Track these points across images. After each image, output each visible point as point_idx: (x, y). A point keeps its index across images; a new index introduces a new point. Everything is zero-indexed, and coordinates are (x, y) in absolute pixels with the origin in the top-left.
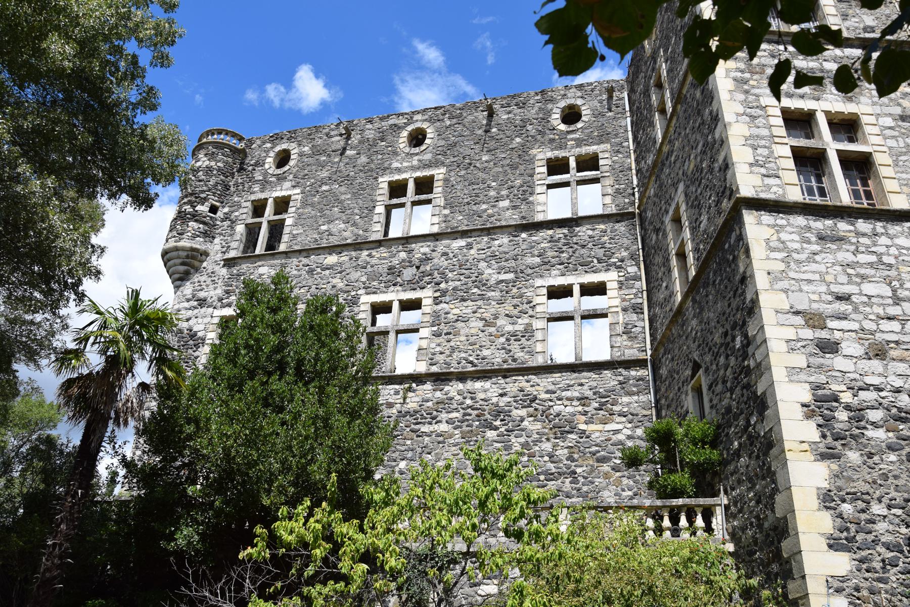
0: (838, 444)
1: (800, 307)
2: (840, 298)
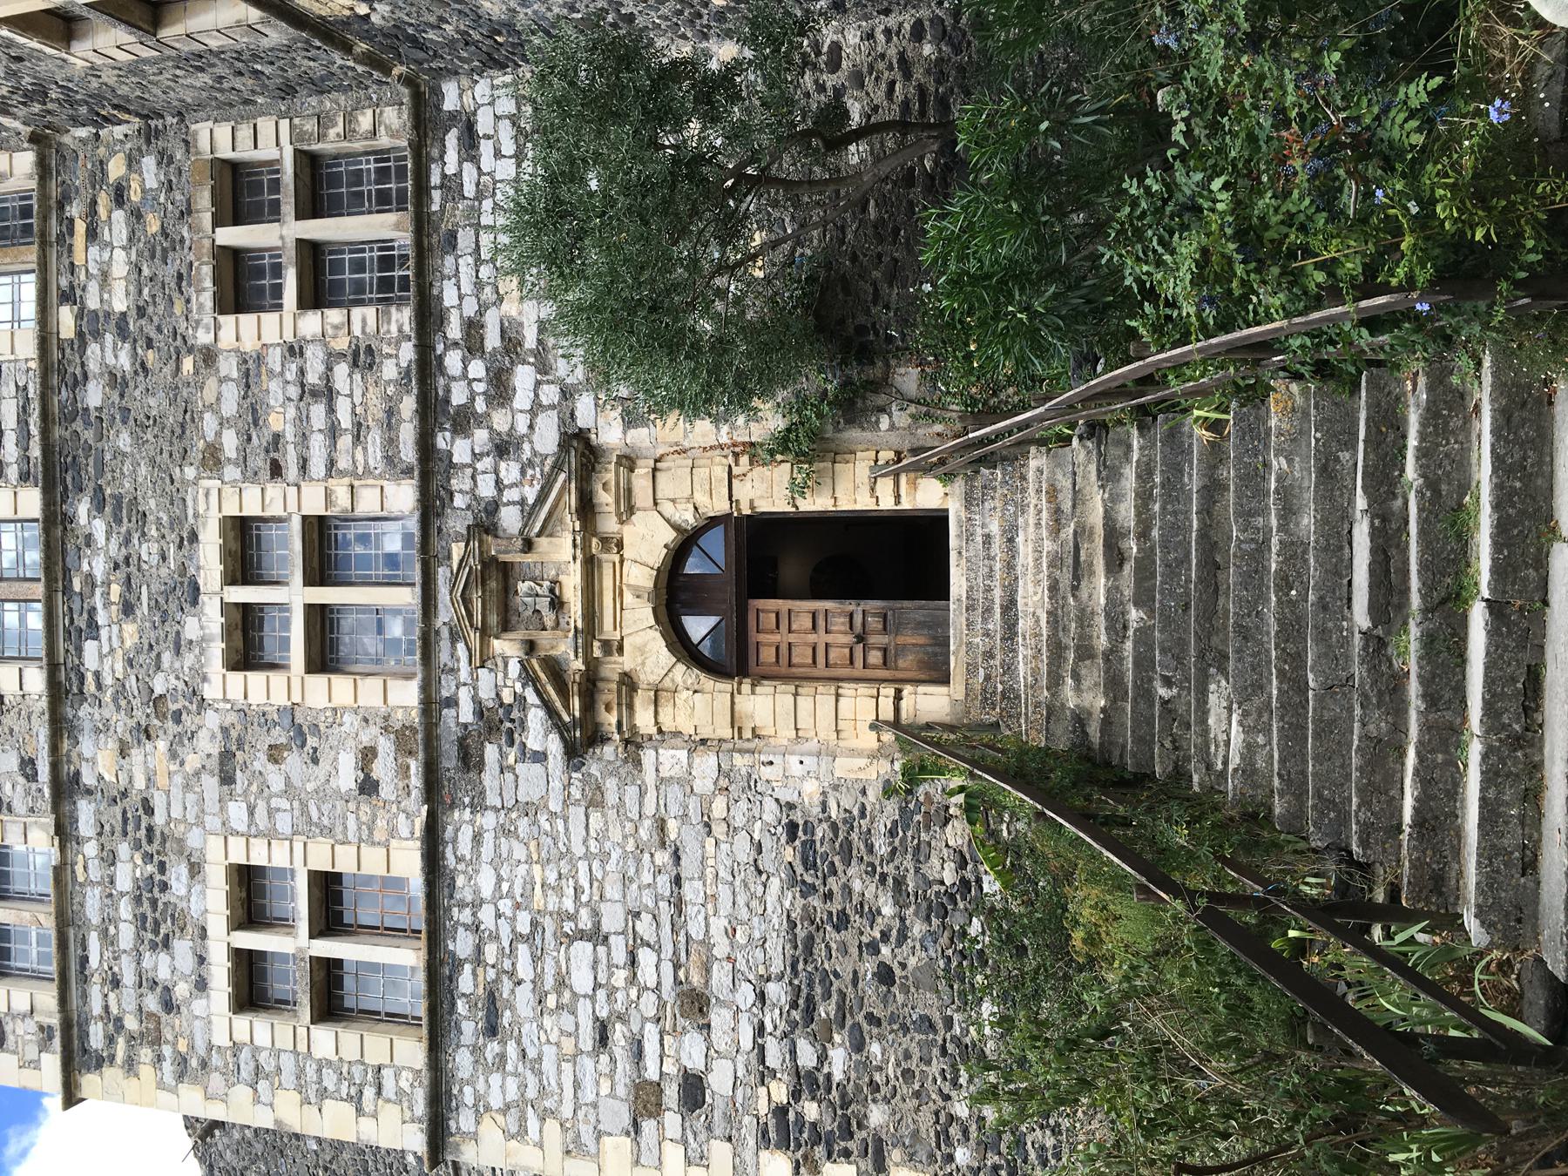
1: (626, 1120)
2: (603, 1039)
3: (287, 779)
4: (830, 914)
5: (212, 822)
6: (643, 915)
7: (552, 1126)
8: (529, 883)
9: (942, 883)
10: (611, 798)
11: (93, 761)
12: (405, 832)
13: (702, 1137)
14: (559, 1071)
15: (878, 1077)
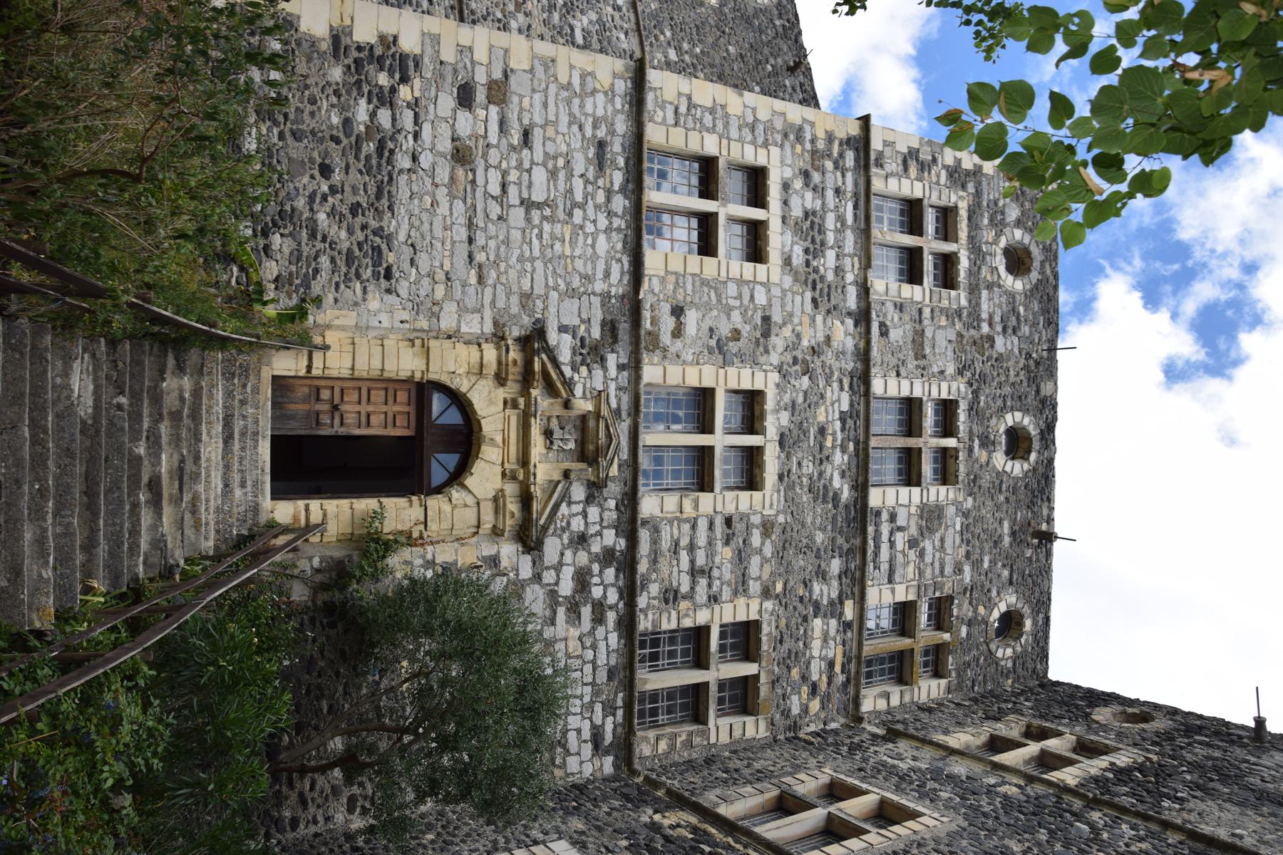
0: (349, 61)
2: (526, 135)
3: (729, 319)
4: (363, 215)
5: (776, 292)
6: (495, 218)
7: (563, 79)
8: (573, 243)
9: (282, 235)
10: (515, 300)
11: (847, 334)
12: (655, 280)
13: (460, 65)
14: (557, 115)
15: (334, 100)
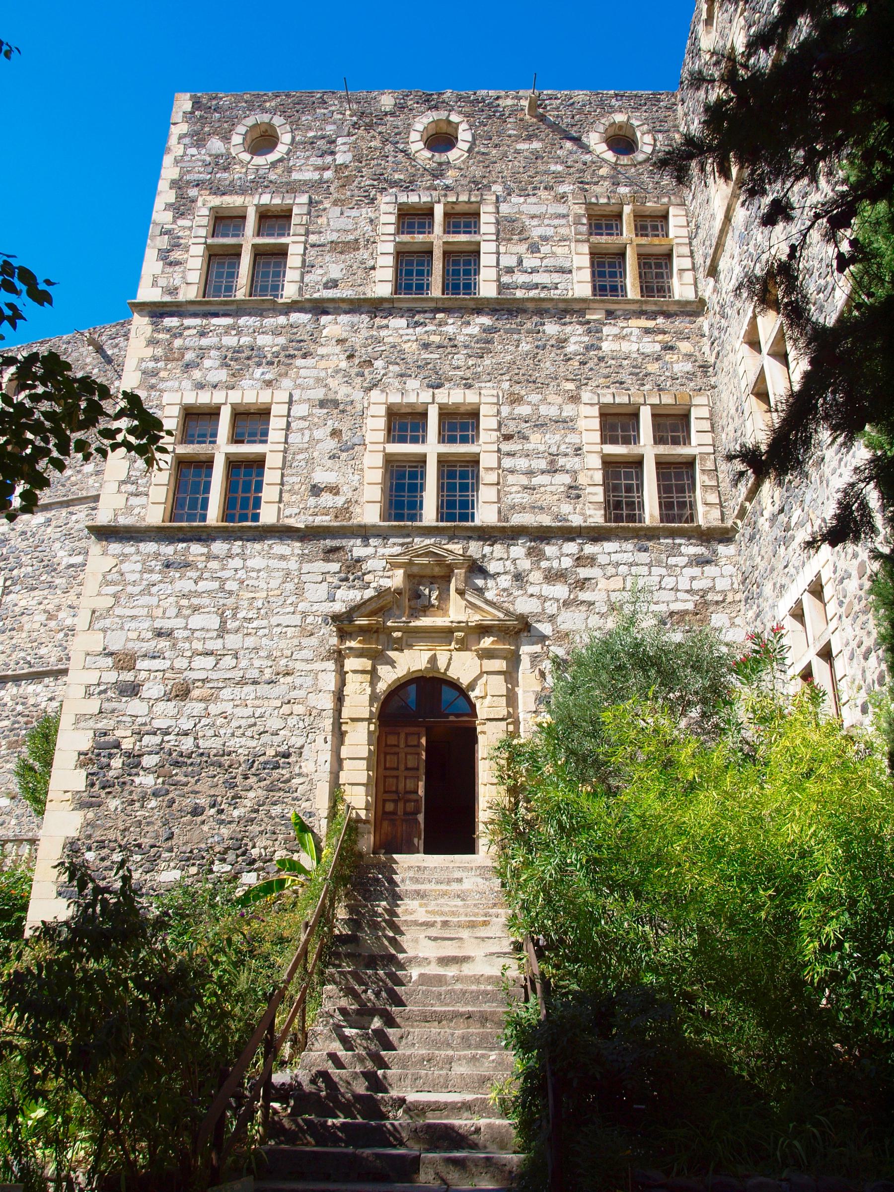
1: (113, 648)
2: (159, 634)
7: (110, 601)
8: (255, 589)
10: (306, 641)
14: (143, 606)
15: (137, 804)
